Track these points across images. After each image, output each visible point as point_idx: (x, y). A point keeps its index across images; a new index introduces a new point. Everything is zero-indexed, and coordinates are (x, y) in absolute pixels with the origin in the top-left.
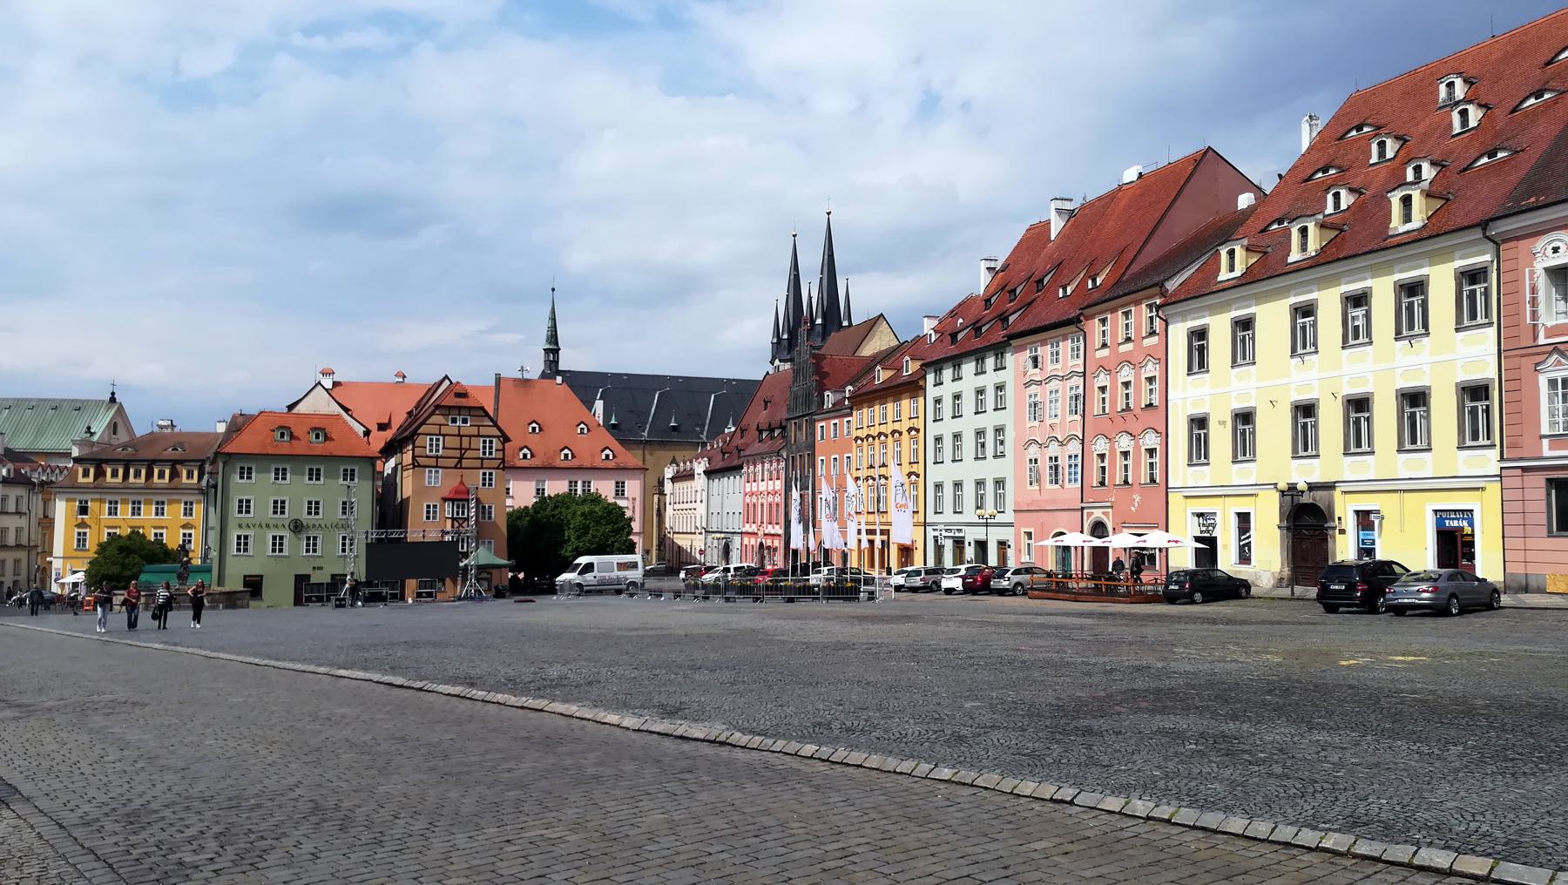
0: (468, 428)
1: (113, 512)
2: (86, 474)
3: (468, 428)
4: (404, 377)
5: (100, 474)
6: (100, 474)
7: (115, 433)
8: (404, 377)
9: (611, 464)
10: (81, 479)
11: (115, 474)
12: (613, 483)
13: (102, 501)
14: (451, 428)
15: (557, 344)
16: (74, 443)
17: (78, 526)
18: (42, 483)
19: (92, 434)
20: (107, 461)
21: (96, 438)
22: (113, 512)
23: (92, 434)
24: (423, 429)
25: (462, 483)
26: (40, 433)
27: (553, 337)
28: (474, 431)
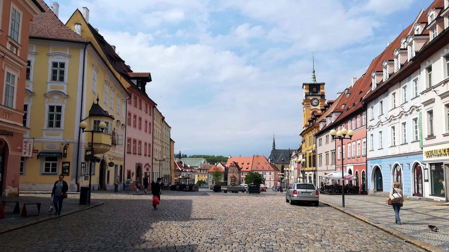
0: (234, 168)
1: (202, 176)
2: (199, 171)
3: (234, 168)
4: (240, 156)
5: (201, 171)
6: (201, 171)
7: (205, 163)
8: (240, 156)
9: (269, 170)
10: (198, 172)
11: (202, 171)
12: (269, 173)
13: (201, 175)
14: (232, 168)
15: (275, 145)
16: (199, 165)
17: (198, 178)
18: (195, 172)
19: (202, 164)
20: (201, 169)
21: (202, 164)
22: (202, 176)
23: (202, 164)
24: (229, 168)
25: (233, 175)
26: (195, 164)
27: (274, 144)
28: (235, 169)
